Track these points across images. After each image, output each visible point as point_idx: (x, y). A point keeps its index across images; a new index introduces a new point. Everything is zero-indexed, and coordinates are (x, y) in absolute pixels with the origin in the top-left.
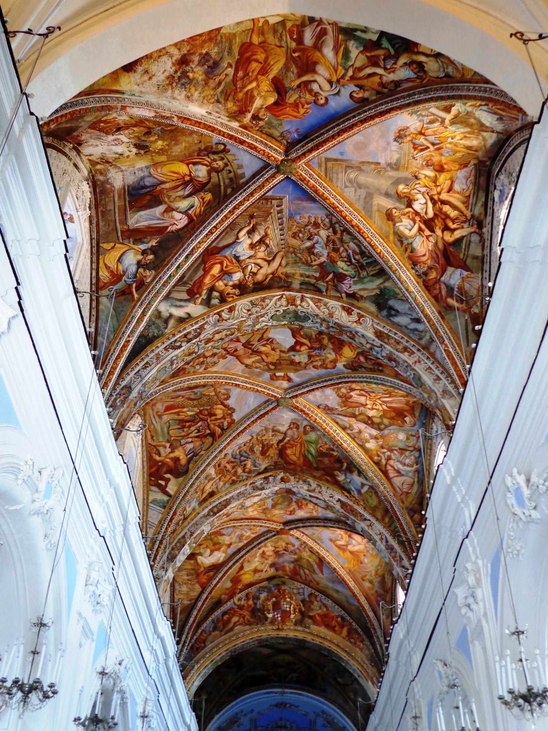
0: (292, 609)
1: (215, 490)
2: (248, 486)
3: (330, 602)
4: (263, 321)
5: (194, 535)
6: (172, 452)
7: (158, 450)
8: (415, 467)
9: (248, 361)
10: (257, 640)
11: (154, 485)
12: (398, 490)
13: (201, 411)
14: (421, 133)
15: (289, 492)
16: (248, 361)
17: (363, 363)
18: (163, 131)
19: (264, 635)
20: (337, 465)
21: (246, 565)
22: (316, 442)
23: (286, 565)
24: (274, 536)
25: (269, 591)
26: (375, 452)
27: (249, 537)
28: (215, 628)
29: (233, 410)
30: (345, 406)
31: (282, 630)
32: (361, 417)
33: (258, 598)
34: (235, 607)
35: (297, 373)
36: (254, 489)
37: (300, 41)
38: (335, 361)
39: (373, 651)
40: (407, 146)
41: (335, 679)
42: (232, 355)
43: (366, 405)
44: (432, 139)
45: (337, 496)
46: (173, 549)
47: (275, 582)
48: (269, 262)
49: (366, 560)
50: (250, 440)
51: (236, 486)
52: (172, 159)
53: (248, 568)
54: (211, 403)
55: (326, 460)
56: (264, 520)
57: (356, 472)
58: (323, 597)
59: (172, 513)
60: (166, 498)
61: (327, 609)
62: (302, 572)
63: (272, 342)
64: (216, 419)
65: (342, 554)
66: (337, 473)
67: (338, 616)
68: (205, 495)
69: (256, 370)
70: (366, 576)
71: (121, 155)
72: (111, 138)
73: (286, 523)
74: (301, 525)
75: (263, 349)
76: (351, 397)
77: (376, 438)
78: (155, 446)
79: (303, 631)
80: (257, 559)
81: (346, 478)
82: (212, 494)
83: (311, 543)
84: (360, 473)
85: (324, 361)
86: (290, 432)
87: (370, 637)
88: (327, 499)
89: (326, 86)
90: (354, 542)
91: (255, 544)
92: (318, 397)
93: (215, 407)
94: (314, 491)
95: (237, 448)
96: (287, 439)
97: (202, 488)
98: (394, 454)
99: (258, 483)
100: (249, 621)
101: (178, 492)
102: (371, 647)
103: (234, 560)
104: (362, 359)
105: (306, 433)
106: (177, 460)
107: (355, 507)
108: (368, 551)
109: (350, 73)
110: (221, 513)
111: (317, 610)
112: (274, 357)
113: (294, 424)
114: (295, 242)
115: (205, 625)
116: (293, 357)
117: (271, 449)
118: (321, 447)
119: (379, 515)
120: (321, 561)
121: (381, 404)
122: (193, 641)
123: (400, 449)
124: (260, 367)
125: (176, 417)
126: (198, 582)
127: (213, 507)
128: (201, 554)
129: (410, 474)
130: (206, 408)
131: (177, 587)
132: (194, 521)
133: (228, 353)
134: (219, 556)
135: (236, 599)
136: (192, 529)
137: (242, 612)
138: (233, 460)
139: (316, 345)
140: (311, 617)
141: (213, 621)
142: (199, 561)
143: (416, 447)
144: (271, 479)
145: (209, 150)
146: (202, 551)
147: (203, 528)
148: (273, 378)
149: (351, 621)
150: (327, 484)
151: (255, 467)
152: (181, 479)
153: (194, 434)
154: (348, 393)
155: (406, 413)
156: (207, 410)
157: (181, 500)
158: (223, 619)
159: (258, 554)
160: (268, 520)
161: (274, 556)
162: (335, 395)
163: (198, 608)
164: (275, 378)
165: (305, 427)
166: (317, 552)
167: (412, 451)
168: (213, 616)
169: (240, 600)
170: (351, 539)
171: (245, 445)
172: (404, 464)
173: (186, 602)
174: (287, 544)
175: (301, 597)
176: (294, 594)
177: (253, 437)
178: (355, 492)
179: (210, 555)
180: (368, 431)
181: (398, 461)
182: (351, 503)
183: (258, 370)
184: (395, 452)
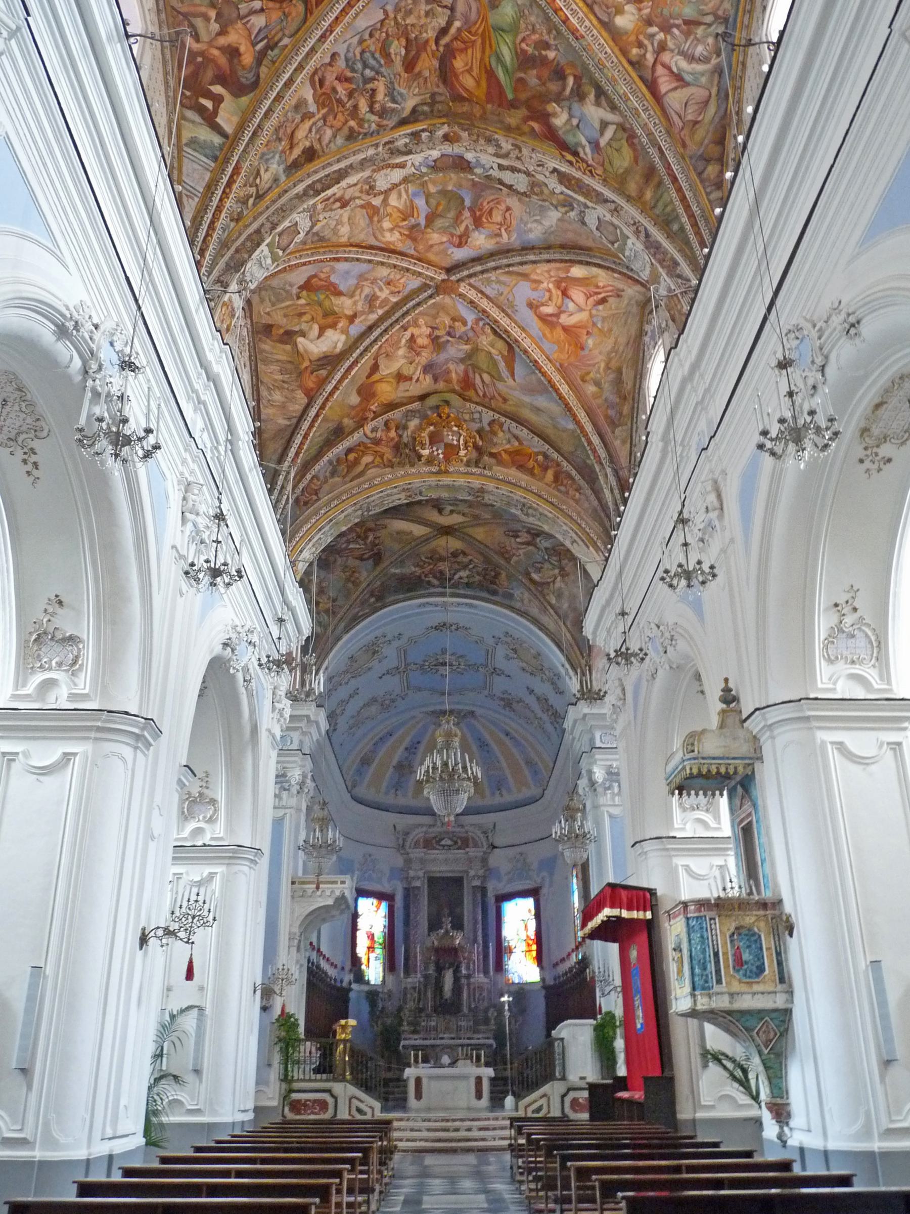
0: (462, 442)
1: (317, 146)
2: (380, 149)
3: (525, 431)
5: (279, 229)
6: (222, 32)
7: (192, 26)
8: (714, 61)
10: (404, 490)
11: (190, 108)
12: (676, 118)
15: (461, 165)
19: (417, 482)
20: (553, 87)
21: (382, 362)
22: (514, 29)
23: (452, 367)
24: (431, 297)
25: (424, 417)
26: (632, 38)
27: (386, 300)
28: (333, 474)
31: (446, 472)
33: (405, 427)
34: (367, 441)
36: (392, 153)
39: (596, 503)
41: (528, 574)
45: (552, 164)
46: (237, 251)
47: (432, 401)
49: (590, 342)
50: (382, 21)
51: (355, 146)
53: (387, 369)
55: (532, 78)
56: (412, 257)
57: (592, 96)
58: (514, 424)
59: (230, 169)
60: (217, 140)
61: (521, 443)
62: (478, 380)
65: (548, 335)
66: (553, 107)
67: (537, 454)
68: (297, 152)
70: (588, 373)
73: (449, 270)
74: (479, 268)
78: (186, 16)
79: (481, 475)
80: (401, 352)
81: (571, 116)
82: (310, 155)
83: (495, 313)
84: (600, 93)
87: (591, 479)
88: (531, 168)
90: (571, 306)
91: (398, 315)
94: (506, 156)
95: (355, 40)
96: (457, 24)
97: (289, 131)
98: (674, 37)
99: (400, 143)
100: (390, 461)
101: (241, 128)
102: (593, 497)
103: (362, 348)
106: (233, 52)
107: (587, 180)
108: (594, 324)
110: (329, 192)
111: (502, 442)
115: (317, 467)
117: (424, 56)
118: (523, 40)
119: (632, 187)
120: (511, 347)
122: (298, 491)
123: (687, 22)
126: (301, 387)
127: (314, 183)
128: (303, 334)
129: (703, 80)
131: (264, 393)
132: (278, 205)
134: (334, 340)
135: (368, 428)
136: (275, 219)
137: (378, 449)
138: (349, 74)
140: (492, 455)
141: (330, 462)
142: (300, 347)
143: (720, 13)
144: (424, 135)
146: (304, 326)
147: (295, 217)
149: (560, 459)
150: (532, 142)
151: (394, 101)
152: (245, 100)
157: (247, 145)
158: (346, 459)
159: (404, 341)
160: (420, 260)
161: (431, 346)
163: (302, 433)
166: (506, 331)
167: (710, 25)
168: (330, 454)
169: (374, 430)
170: (567, 300)
171: (371, 35)
172: (691, 59)
173: (283, 422)
174: (454, 319)
175: (477, 426)
176: (465, 421)
177: (386, 12)
178: (588, 150)
179: (320, 336)
181: (682, 53)
182: (578, 174)
184: (675, 31)
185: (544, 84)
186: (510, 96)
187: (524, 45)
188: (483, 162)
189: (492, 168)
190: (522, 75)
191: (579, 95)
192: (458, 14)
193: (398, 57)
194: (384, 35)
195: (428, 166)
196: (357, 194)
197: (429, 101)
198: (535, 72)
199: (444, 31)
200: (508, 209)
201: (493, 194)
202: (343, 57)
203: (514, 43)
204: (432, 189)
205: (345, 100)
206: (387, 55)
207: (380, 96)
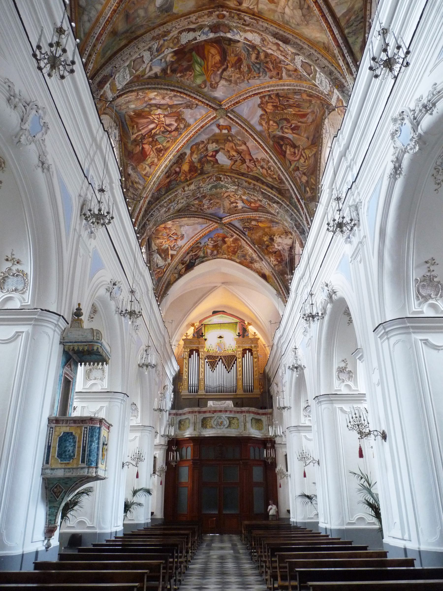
4: (233, 189)
9: (243, 147)
13: (283, 110)
14: (175, 240)
16: (243, 147)
17: (177, 167)
18: (262, 245)
20: (175, 66)
22: (195, 77)
29: (259, 106)
30: (178, 112)
32: (165, 107)
35: (213, 133)
37: (218, 252)
40: (179, 233)
42: (253, 159)
43: (164, 117)
44: (172, 239)
48: (229, 196)
50: (250, 79)
52: (263, 229)
54: (274, 114)
57: (158, 74)
63: (229, 157)
64: (272, 102)
71: (280, 237)
72: (280, 248)
75: (235, 154)
76: (176, 121)
77: (151, 99)
85: (198, 150)
86: (217, 79)
89: (209, 243)
92: (198, 114)
95: (261, 78)
96: (219, 72)
104: (178, 169)
105: (205, 82)
109: (202, 249)
112: (228, 146)
113: (215, 88)
114: (218, 201)
116: (217, 146)
117: (233, 62)
118: (191, 75)
124: (237, 140)
125: (301, 110)
130: (278, 112)
133: (254, 162)
138: (266, 69)
139: (204, 160)
145: (249, 229)
148: (229, 128)
153: (292, 100)
154: (178, 125)
155: (135, 116)
156: (278, 110)
162: (187, 119)
164: (228, 127)
165: (205, 86)
171: (255, 77)
180: (157, 101)
183: (239, 138)
185: (179, 65)
186: (194, 53)
187: (191, 73)
189: (199, 36)
191: (164, 71)
192: (219, 76)
193: (244, 65)
194: (249, 75)
195: (233, 31)
196: (270, 44)
197: (232, 42)
198: (184, 67)
199: (224, 70)
202: (268, 76)
203: (194, 72)
205: (269, 62)
206: (249, 68)
207: (254, 56)
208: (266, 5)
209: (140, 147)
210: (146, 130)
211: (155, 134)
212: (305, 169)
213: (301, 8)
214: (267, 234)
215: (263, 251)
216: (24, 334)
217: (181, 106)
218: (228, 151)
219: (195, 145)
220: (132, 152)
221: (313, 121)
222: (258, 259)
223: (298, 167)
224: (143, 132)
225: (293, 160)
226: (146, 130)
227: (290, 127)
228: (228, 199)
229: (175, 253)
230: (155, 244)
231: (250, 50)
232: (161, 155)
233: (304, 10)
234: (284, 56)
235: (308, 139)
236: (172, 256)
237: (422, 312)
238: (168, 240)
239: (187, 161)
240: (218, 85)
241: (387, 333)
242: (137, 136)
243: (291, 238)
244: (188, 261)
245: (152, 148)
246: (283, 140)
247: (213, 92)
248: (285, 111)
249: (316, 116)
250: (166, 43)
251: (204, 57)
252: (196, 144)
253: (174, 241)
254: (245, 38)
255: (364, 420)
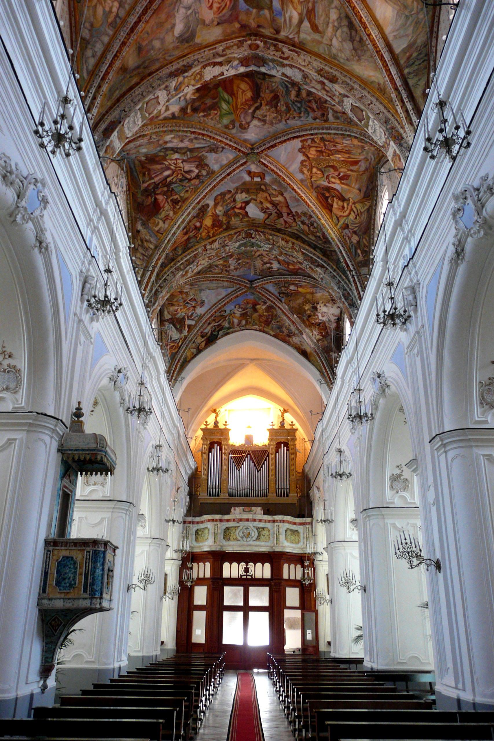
9: (280, 198)
14: (194, 307)
16: (280, 198)
17: (197, 221)
20: (197, 104)
22: (221, 117)
29: (300, 150)
30: (200, 157)
32: (184, 151)
35: (243, 181)
37: (247, 321)
38: (216, 205)
40: (198, 299)
42: (292, 212)
43: (182, 162)
44: (189, 306)
48: (262, 255)
50: (288, 119)
52: (304, 295)
54: (318, 160)
55: (209, 102)
57: (176, 114)
64: (316, 147)
69: (276, 188)
72: (324, 319)
75: (269, 205)
76: (197, 167)
77: (166, 142)
85: (224, 202)
86: (249, 120)
89: (236, 312)
92: (224, 158)
93: (315, 157)
95: (302, 119)
96: (250, 111)
104: (198, 224)
105: (233, 122)
112: (261, 196)
113: (245, 128)
114: (247, 261)
116: (247, 196)
117: (269, 99)
121: (170, 165)
133: (293, 216)
138: (309, 109)
139: (230, 212)
145: (287, 295)
148: (262, 176)
153: (340, 145)
154: (200, 171)
162: (210, 165)
164: (262, 175)
171: (294, 117)
183: (274, 187)
186: (220, 89)
187: (216, 112)
188: (234, 70)
190: (214, 101)
191: (183, 110)
192: (250, 115)
196: (314, 82)
199: (258, 108)
200: (211, 7)
201: (224, 15)
202: (310, 117)
203: (220, 111)
204: (266, 12)
207: (293, 93)
208: (309, 34)
209: (152, 197)
210: (159, 177)
211: (171, 183)
212: (356, 227)
213: (352, 40)
214: (309, 302)
215: (303, 321)
216: (17, 442)
217: (204, 149)
218: (261, 203)
219: (220, 195)
220: (143, 205)
221: (366, 169)
222: (296, 332)
223: (347, 225)
224: (156, 179)
225: (341, 216)
226: (159, 177)
227: (337, 176)
228: (261, 258)
229: (193, 323)
230: (168, 312)
231: (289, 86)
232: (178, 207)
233: (356, 43)
234: (330, 97)
235: (360, 191)
236: (189, 326)
237: (486, 422)
238: (185, 307)
239: (210, 214)
240: (249, 126)
241: (444, 445)
242: (149, 185)
243: (338, 307)
244: (209, 333)
245: (166, 200)
246: (329, 192)
247: (243, 133)
248: (332, 157)
249: (370, 164)
250: (186, 80)
251: (232, 94)
252: (221, 194)
253: (192, 309)
254: (283, 74)
255: (416, 547)
